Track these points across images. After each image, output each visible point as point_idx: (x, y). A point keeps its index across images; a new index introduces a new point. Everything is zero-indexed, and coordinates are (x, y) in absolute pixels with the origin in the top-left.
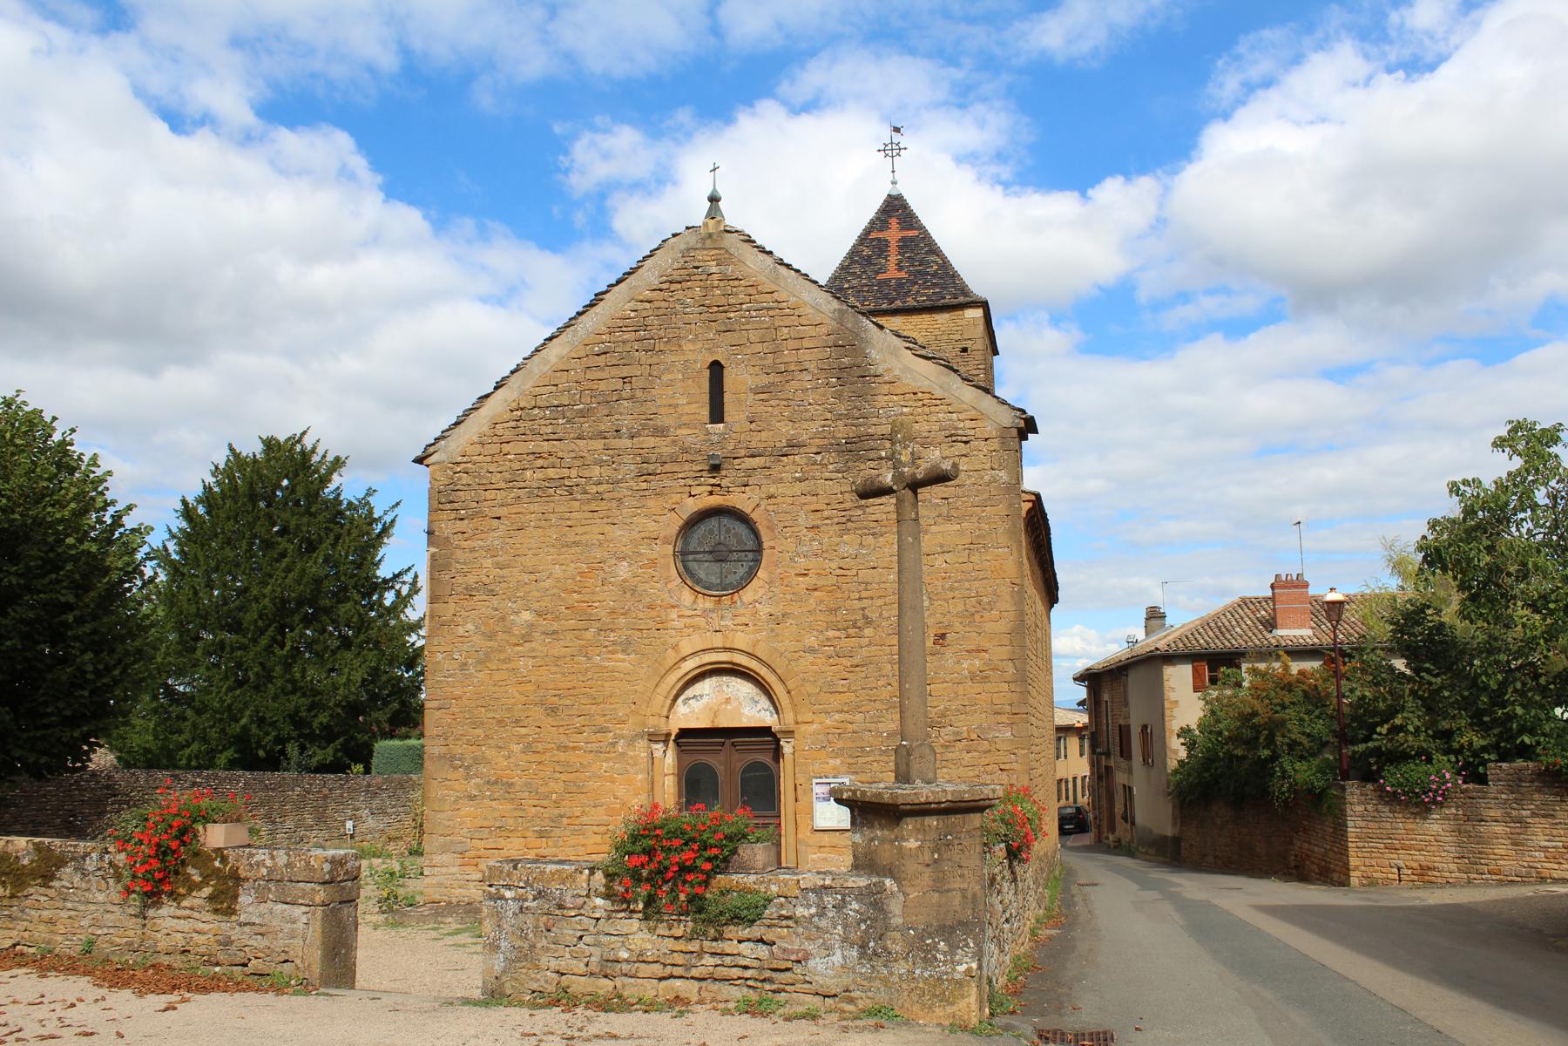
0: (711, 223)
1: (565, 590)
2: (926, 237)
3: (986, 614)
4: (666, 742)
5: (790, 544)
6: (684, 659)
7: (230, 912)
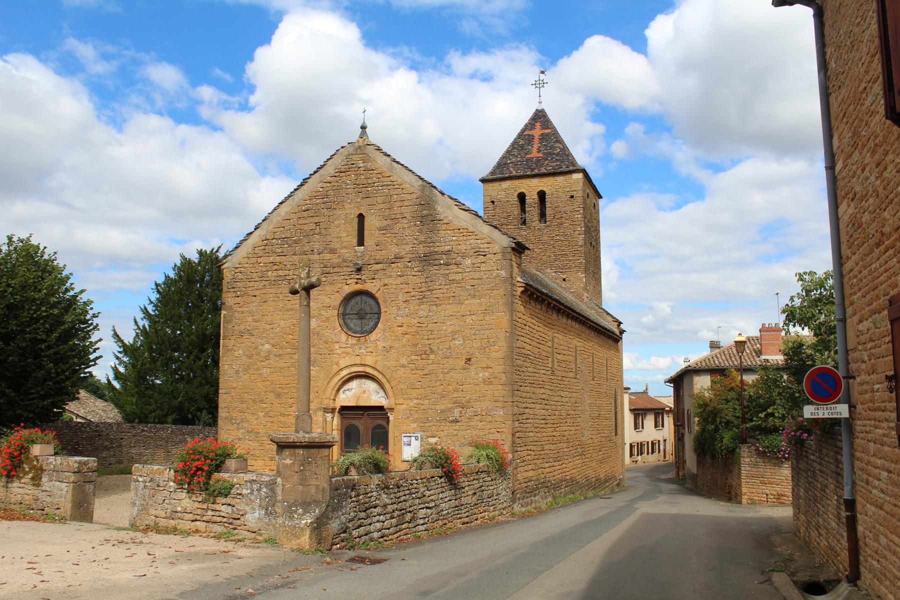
0: (361, 140)
1: (286, 334)
2: (555, 133)
3: (492, 348)
5: (394, 310)
6: (341, 370)
7: (38, 485)
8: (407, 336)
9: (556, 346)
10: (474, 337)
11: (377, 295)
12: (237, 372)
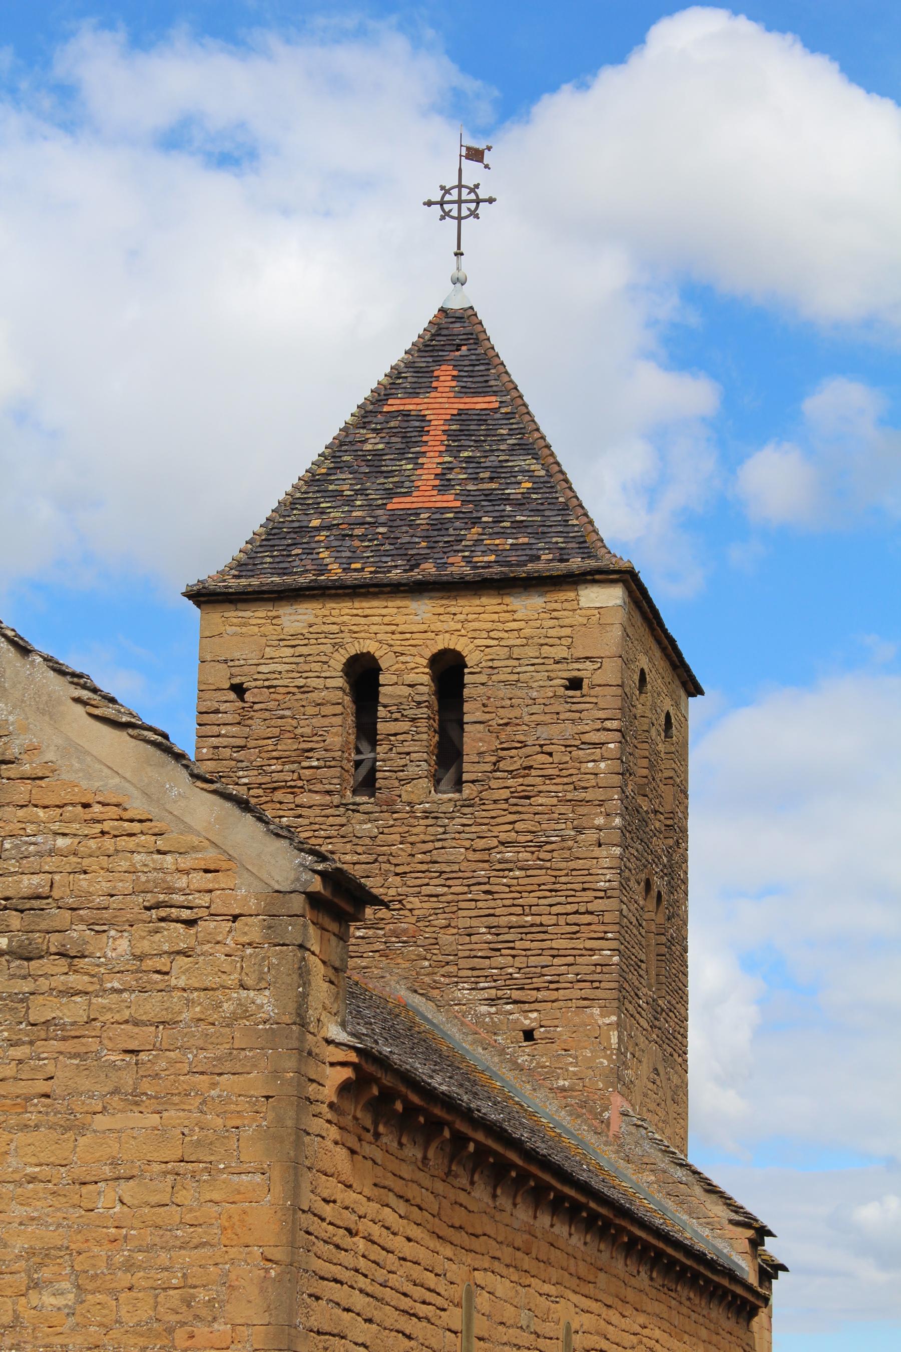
3: (201, 1330)
9: (480, 1326)
10: (125, 1279)
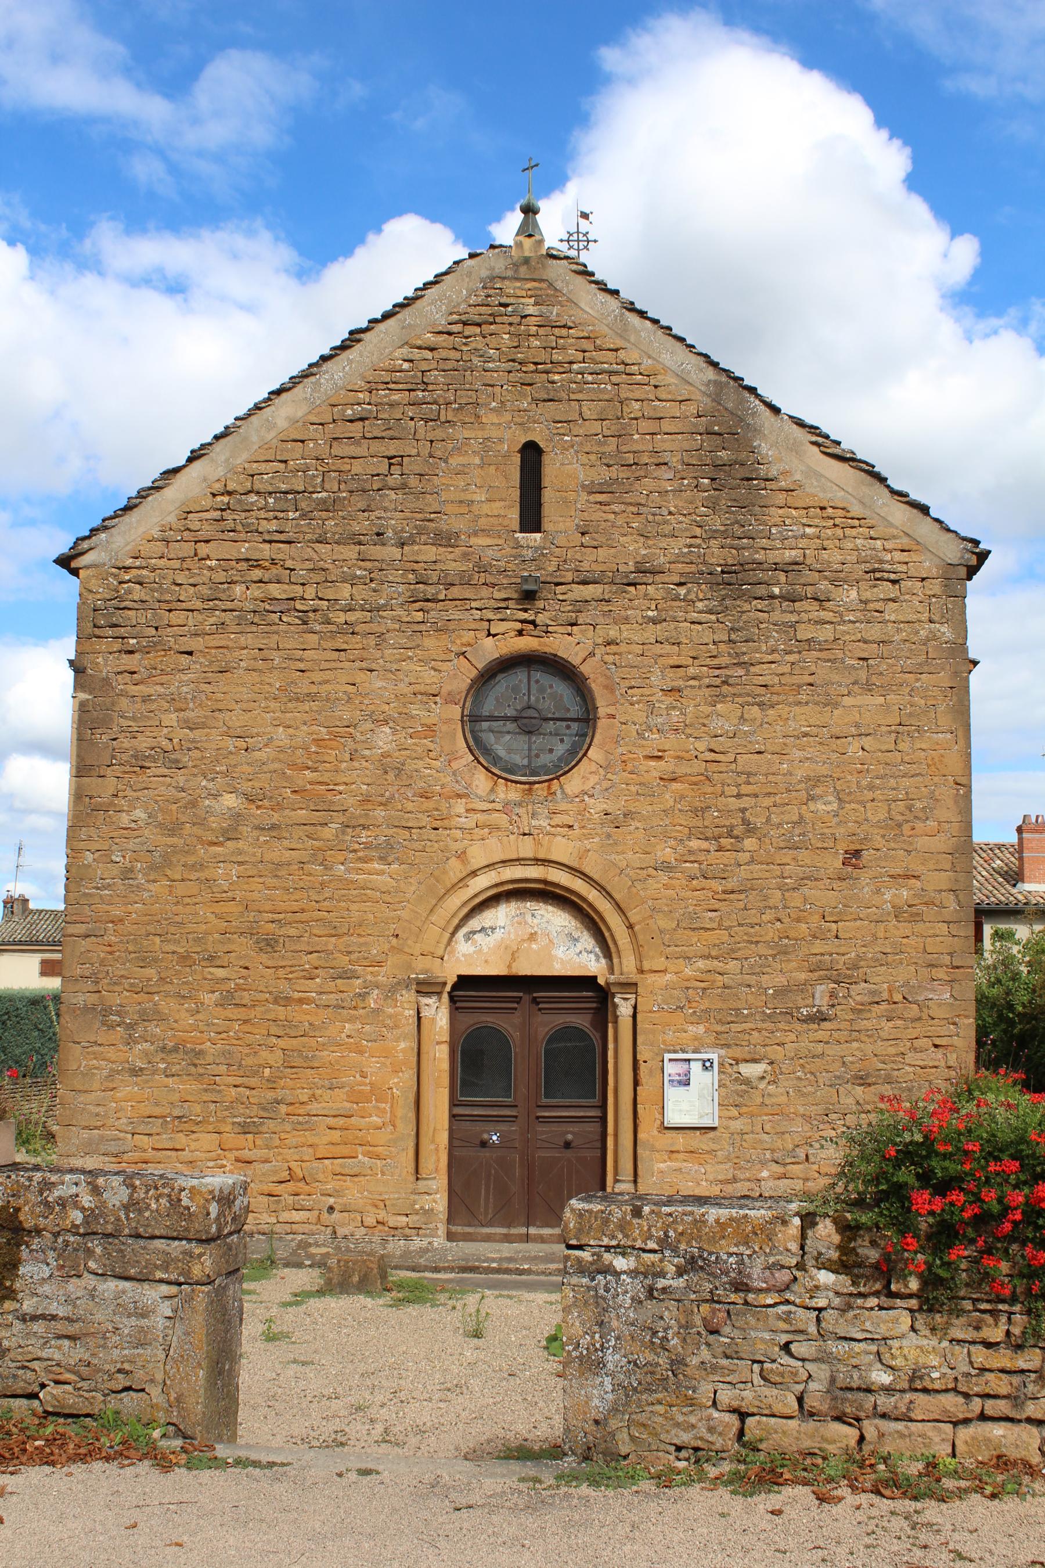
0: (528, 243)
1: (293, 766)
3: (919, 825)
4: (439, 994)
6: (474, 873)
8: (675, 786)
10: (870, 795)
11: (585, 669)
12: (127, 874)
